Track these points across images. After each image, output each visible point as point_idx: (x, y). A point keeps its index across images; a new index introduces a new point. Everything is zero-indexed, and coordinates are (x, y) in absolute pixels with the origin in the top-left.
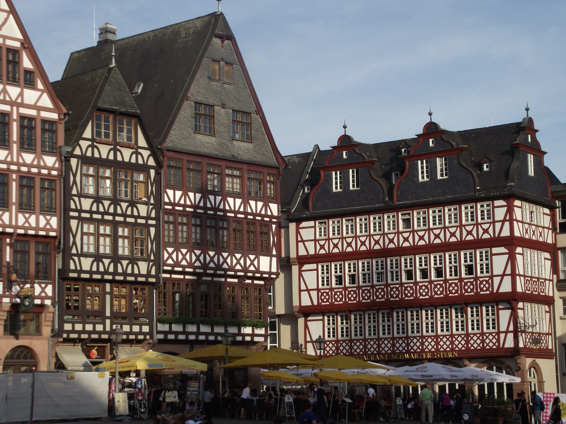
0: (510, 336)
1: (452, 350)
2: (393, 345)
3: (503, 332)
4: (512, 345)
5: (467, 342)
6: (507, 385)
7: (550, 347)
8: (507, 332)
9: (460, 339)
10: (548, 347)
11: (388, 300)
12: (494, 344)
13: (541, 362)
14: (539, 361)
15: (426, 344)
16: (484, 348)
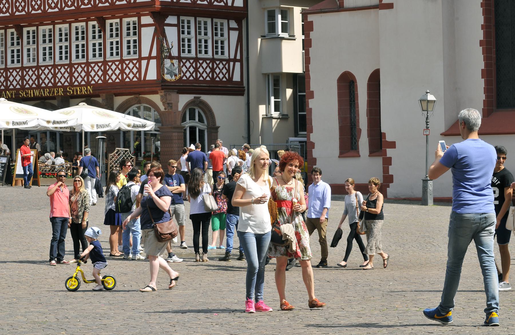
0: (153, 63)
1: (88, 83)
2: (23, 78)
3: (145, 58)
4: (155, 78)
5: (105, 72)
6: (5, 131)
7: (237, 78)
8: (149, 58)
9: (96, 68)
10: (231, 79)
11: (13, 14)
12: (135, 76)
13: (212, 101)
14: (205, 98)
15: (59, 75)
16: (123, 80)
